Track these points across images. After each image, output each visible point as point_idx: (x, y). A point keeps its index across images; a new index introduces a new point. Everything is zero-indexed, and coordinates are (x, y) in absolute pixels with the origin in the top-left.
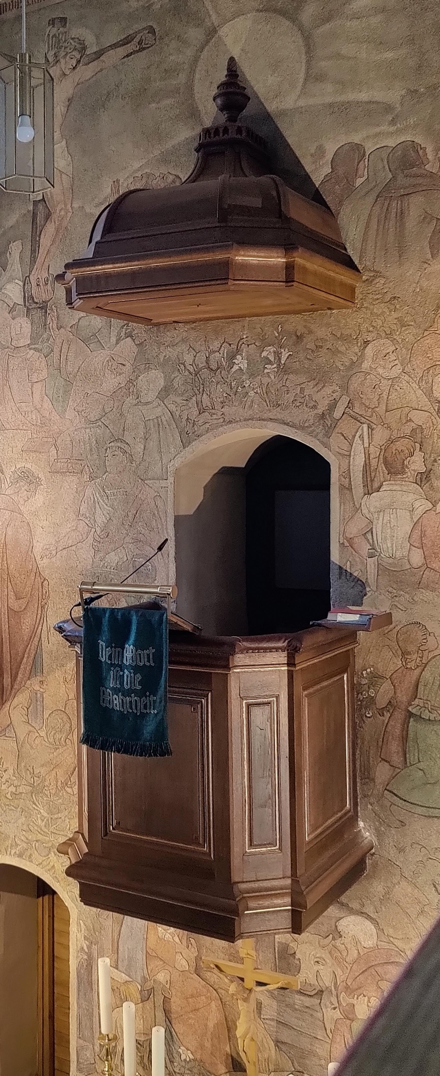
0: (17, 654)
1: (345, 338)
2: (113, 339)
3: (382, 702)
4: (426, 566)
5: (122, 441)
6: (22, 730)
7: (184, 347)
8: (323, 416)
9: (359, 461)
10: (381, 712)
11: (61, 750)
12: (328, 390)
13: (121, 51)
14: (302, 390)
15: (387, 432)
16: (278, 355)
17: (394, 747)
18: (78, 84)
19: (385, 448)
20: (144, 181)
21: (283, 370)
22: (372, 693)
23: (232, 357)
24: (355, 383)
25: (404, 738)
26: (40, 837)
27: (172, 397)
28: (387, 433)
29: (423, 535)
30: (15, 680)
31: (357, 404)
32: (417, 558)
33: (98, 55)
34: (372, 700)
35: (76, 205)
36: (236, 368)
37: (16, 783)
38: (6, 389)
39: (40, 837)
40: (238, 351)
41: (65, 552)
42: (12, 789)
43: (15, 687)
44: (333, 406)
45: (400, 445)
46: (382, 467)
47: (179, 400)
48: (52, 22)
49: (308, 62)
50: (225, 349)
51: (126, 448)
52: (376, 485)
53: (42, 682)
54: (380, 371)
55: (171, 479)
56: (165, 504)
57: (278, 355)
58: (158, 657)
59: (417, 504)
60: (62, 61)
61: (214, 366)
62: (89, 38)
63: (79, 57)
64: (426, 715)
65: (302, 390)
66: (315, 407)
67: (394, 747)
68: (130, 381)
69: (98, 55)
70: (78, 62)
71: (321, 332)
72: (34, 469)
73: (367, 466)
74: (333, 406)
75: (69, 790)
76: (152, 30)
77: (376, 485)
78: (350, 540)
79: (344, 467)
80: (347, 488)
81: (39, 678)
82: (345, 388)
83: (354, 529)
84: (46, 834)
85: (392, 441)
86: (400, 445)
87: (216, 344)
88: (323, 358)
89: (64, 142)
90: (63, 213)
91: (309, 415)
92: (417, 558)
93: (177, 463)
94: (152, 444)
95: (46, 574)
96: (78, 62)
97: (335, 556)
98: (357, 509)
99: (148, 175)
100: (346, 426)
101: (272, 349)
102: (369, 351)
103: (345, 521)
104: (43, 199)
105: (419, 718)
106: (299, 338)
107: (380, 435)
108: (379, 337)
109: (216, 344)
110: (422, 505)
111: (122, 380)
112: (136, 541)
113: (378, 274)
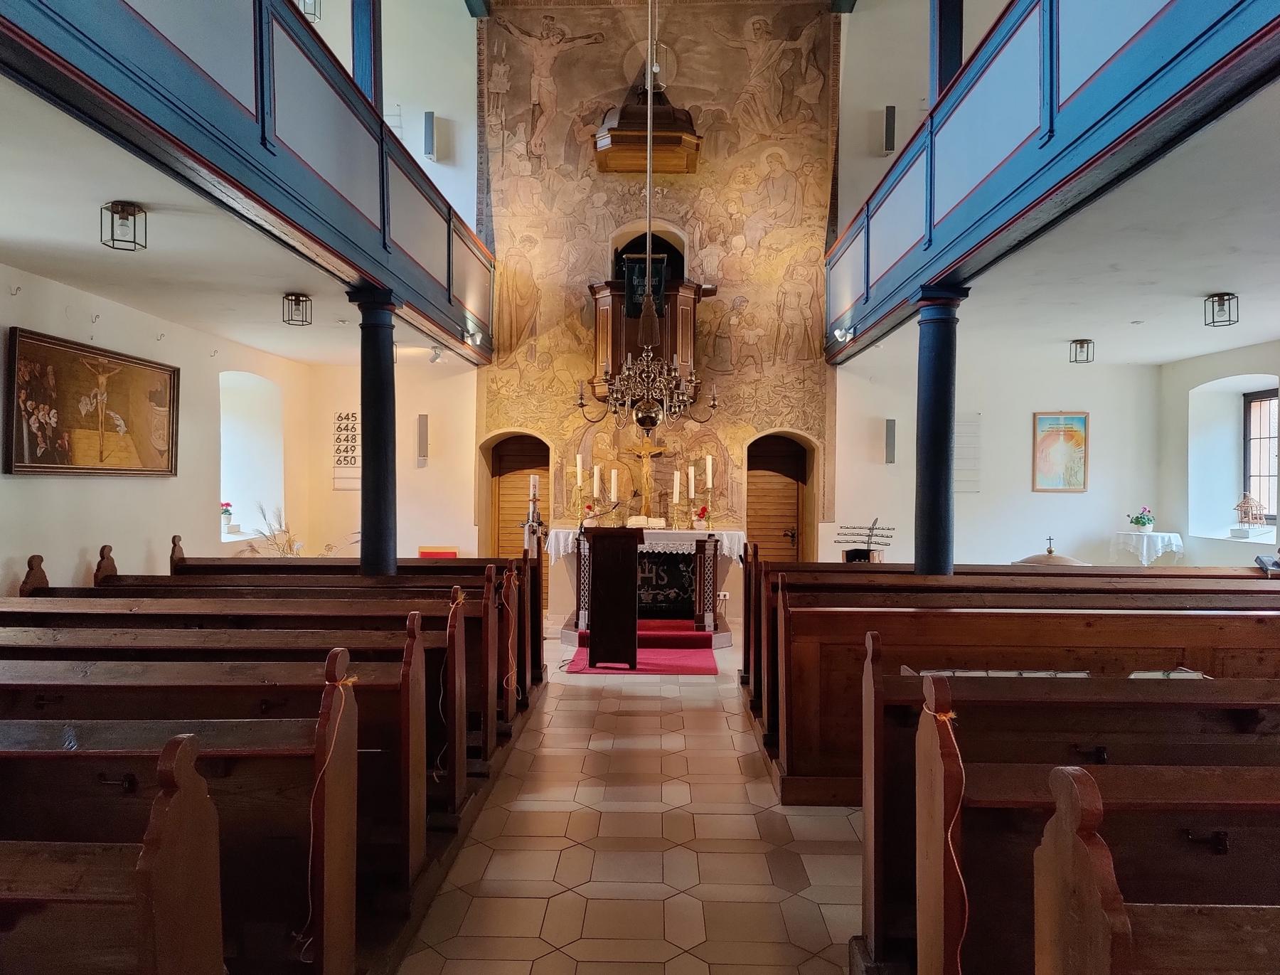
0: (521, 327)
1: (693, 186)
2: (579, 177)
3: (705, 333)
5: (584, 224)
6: (522, 365)
7: (617, 183)
9: (697, 236)
11: (546, 371)
12: (685, 207)
13: (586, 41)
14: (673, 206)
15: (709, 225)
16: (662, 191)
17: (710, 350)
18: (560, 51)
20: (597, 104)
22: (701, 329)
23: (641, 190)
24: (696, 205)
25: (714, 345)
26: (532, 415)
27: (610, 206)
28: (709, 225)
30: (520, 338)
31: (697, 213)
33: (573, 40)
34: (702, 331)
36: (642, 194)
37: (518, 391)
38: (517, 196)
39: (532, 415)
40: (644, 188)
42: (516, 394)
43: (519, 343)
45: (714, 230)
46: (707, 239)
47: (614, 206)
48: (546, 17)
49: (678, 70)
50: (638, 186)
51: (586, 227)
52: (704, 246)
53: (535, 340)
55: (610, 242)
56: (607, 252)
60: (552, 38)
62: (567, 31)
63: (561, 38)
64: (723, 336)
65: (673, 206)
66: (679, 213)
67: (710, 350)
68: (589, 197)
69: (573, 40)
70: (561, 41)
71: (681, 183)
72: (534, 236)
73: (701, 238)
75: (551, 390)
77: (704, 246)
78: (693, 268)
79: (691, 239)
81: (534, 338)
82: (692, 206)
84: (536, 413)
85: (711, 228)
86: (714, 230)
87: (633, 184)
88: (682, 193)
89: (552, 78)
90: (551, 112)
91: (676, 217)
92: (720, 275)
93: (613, 235)
94: (600, 226)
95: (540, 287)
96: (561, 41)
97: (686, 275)
99: (599, 102)
100: (692, 222)
101: (660, 188)
103: (691, 261)
104: (539, 104)
106: (672, 184)
107: (707, 226)
108: (706, 186)
109: (633, 184)
110: (723, 254)
111: (584, 196)
112: (591, 270)
113: (707, 161)
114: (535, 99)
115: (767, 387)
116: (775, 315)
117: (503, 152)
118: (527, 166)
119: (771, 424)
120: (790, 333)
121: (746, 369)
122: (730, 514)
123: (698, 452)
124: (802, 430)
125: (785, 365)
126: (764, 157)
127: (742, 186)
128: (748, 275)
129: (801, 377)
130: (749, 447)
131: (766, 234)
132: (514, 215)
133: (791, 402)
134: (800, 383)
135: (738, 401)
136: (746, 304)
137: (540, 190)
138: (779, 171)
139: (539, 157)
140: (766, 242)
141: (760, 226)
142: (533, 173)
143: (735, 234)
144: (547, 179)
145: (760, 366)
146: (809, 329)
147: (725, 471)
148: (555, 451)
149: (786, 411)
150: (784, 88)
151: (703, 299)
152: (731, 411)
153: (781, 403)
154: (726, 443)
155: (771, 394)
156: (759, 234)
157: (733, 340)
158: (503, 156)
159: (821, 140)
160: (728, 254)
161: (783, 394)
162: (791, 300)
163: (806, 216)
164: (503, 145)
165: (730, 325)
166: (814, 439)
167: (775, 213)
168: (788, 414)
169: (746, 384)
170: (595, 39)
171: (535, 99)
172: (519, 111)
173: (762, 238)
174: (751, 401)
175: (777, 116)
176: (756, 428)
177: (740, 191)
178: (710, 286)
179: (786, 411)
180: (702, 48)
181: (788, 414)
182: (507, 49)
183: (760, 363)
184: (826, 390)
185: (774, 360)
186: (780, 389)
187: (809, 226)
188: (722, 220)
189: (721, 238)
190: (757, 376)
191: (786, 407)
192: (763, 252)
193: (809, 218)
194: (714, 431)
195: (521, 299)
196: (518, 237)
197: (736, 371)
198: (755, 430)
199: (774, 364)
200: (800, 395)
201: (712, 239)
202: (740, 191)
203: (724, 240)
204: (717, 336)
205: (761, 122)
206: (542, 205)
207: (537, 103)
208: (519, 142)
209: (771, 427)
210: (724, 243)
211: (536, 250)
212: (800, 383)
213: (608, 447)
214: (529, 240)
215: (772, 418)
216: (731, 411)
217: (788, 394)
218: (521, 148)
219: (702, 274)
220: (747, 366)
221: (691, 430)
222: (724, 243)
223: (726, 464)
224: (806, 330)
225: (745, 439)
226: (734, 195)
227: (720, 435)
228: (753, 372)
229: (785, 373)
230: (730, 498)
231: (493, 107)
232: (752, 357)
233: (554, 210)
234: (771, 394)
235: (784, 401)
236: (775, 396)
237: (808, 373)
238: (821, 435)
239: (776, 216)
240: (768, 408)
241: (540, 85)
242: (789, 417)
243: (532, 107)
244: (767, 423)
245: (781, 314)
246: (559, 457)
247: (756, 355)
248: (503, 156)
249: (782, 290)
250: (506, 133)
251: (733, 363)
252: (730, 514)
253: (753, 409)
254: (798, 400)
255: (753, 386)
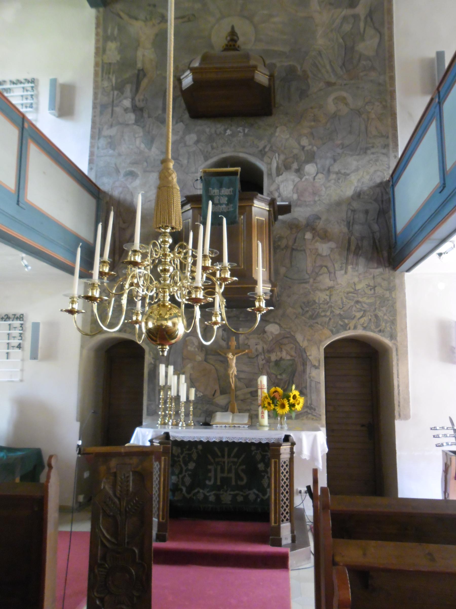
4: (298, 199)
8: (261, 151)
9: (274, 165)
10: (283, 250)
16: (244, 130)
19: (284, 161)
21: (245, 135)
22: (279, 243)
29: (297, 189)
32: (295, 196)
35: (158, 72)
41: (149, 203)
44: (265, 147)
46: (283, 168)
48: (149, 5)
54: (282, 136)
57: (244, 130)
58: (234, 192)
59: (295, 179)
61: (218, 132)
64: (299, 249)
74: (265, 147)
76: (194, 15)
77: (281, 173)
80: (270, 175)
82: (269, 141)
83: (273, 188)
85: (286, 159)
92: (295, 196)
98: (274, 181)
102: (278, 130)
105: (296, 250)
107: (282, 157)
110: (297, 179)
114: (139, 65)
115: (340, 294)
116: (345, 230)
117: (113, 106)
118: (131, 117)
119: (345, 327)
120: (360, 245)
121: (321, 277)
122: (309, 411)
123: (279, 353)
124: (374, 332)
125: (356, 273)
126: (330, 100)
127: (313, 123)
128: (320, 196)
129: (372, 284)
130: (326, 349)
131: (335, 161)
132: (120, 155)
133: (363, 307)
134: (371, 290)
135: (314, 307)
136: (318, 221)
137: (141, 134)
138: (344, 110)
139: (141, 110)
140: (336, 168)
141: (329, 155)
142: (137, 122)
143: (308, 161)
144: (147, 126)
145: (333, 275)
146: (377, 241)
147: (304, 371)
148: (150, 354)
149: (358, 315)
150: (346, 46)
151: (280, 217)
152: (308, 315)
153: (354, 308)
154: (304, 344)
155: (345, 300)
156: (328, 162)
157: (308, 252)
158: (112, 110)
159: (379, 84)
160: (301, 179)
161: (356, 299)
162: (361, 217)
163: (371, 145)
164: (113, 102)
165: (304, 239)
166: (387, 341)
167: (342, 144)
168: (362, 317)
169: (321, 290)
170: (189, 19)
171: (139, 65)
172: (127, 75)
173: (331, 165)
174: (326, 306)
175: (341, 68)
176: (332, 331)
177: (311, 127)
178: (287, 203)
179: (358, 315)
180: (275, 20)
181: (362, 317)
182: (119, 30)
183: (333, 272)
184: (395, 295)
185: (346, 269)
186: (353, 295)
187: (373, 153)
188: (295, 151)
189: (295, 166)
190: (331, 284)
191: (358, 311)
192: (333, 176)
193: (373, 147)
194: (292, 333)
195: (124, 222)
196: (122, 172)
197: (311, 280)
198: (330, 332)
199: (346, 273)
200: (371, 300)
201: (287, 167)
202: (311, 127)
203: (297, 168)
204: (293, 249)
205: (327, 72)
206: (143, 146)
207: (141, 68)
208: (126, 98)
209: (346, 330)
210: (298, 171)
211: (137, 182)
212: (371, 290)
213: (196, 349)
214: (132, 174)
215: (346, 321)
216: (308, 315)
217: (360, 299)
218: (127, 103)
219: (279, 197)
220: (321, 275)
221: (272, 333)
222: (298, 171)
223: (304, 364)
224: (374, 242)
225: (321, 341)
226: (306, 131)
227: (299, 337)
228: (327, 280)
229: (356, 280)
230: (309, 396)
231: (106, 74)
232: (326, 267)
233: (154, 149)
234: (345, 300)
235: (358, 306)
236: (348, 301)
237: (379, 280)
238: (392, 337)
239: (343, 146)
240: (342, 313)
241: (144, 56)
242: (362, 320)
243: (136, 72)
244: (342, 326)
245: (351, 228)
246: (153, 358)
247: (329, 264)
248: (112, 110)
249: (351, 208)
250: (116, 93)
251: (309, 272)
252: (309, 411)
253: (328, 314)
254: (370, 305)
255: (328, 292)
